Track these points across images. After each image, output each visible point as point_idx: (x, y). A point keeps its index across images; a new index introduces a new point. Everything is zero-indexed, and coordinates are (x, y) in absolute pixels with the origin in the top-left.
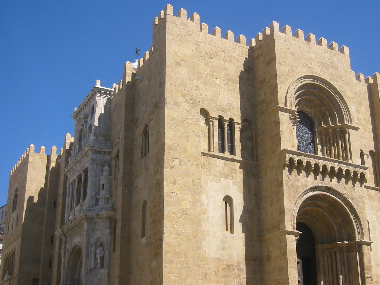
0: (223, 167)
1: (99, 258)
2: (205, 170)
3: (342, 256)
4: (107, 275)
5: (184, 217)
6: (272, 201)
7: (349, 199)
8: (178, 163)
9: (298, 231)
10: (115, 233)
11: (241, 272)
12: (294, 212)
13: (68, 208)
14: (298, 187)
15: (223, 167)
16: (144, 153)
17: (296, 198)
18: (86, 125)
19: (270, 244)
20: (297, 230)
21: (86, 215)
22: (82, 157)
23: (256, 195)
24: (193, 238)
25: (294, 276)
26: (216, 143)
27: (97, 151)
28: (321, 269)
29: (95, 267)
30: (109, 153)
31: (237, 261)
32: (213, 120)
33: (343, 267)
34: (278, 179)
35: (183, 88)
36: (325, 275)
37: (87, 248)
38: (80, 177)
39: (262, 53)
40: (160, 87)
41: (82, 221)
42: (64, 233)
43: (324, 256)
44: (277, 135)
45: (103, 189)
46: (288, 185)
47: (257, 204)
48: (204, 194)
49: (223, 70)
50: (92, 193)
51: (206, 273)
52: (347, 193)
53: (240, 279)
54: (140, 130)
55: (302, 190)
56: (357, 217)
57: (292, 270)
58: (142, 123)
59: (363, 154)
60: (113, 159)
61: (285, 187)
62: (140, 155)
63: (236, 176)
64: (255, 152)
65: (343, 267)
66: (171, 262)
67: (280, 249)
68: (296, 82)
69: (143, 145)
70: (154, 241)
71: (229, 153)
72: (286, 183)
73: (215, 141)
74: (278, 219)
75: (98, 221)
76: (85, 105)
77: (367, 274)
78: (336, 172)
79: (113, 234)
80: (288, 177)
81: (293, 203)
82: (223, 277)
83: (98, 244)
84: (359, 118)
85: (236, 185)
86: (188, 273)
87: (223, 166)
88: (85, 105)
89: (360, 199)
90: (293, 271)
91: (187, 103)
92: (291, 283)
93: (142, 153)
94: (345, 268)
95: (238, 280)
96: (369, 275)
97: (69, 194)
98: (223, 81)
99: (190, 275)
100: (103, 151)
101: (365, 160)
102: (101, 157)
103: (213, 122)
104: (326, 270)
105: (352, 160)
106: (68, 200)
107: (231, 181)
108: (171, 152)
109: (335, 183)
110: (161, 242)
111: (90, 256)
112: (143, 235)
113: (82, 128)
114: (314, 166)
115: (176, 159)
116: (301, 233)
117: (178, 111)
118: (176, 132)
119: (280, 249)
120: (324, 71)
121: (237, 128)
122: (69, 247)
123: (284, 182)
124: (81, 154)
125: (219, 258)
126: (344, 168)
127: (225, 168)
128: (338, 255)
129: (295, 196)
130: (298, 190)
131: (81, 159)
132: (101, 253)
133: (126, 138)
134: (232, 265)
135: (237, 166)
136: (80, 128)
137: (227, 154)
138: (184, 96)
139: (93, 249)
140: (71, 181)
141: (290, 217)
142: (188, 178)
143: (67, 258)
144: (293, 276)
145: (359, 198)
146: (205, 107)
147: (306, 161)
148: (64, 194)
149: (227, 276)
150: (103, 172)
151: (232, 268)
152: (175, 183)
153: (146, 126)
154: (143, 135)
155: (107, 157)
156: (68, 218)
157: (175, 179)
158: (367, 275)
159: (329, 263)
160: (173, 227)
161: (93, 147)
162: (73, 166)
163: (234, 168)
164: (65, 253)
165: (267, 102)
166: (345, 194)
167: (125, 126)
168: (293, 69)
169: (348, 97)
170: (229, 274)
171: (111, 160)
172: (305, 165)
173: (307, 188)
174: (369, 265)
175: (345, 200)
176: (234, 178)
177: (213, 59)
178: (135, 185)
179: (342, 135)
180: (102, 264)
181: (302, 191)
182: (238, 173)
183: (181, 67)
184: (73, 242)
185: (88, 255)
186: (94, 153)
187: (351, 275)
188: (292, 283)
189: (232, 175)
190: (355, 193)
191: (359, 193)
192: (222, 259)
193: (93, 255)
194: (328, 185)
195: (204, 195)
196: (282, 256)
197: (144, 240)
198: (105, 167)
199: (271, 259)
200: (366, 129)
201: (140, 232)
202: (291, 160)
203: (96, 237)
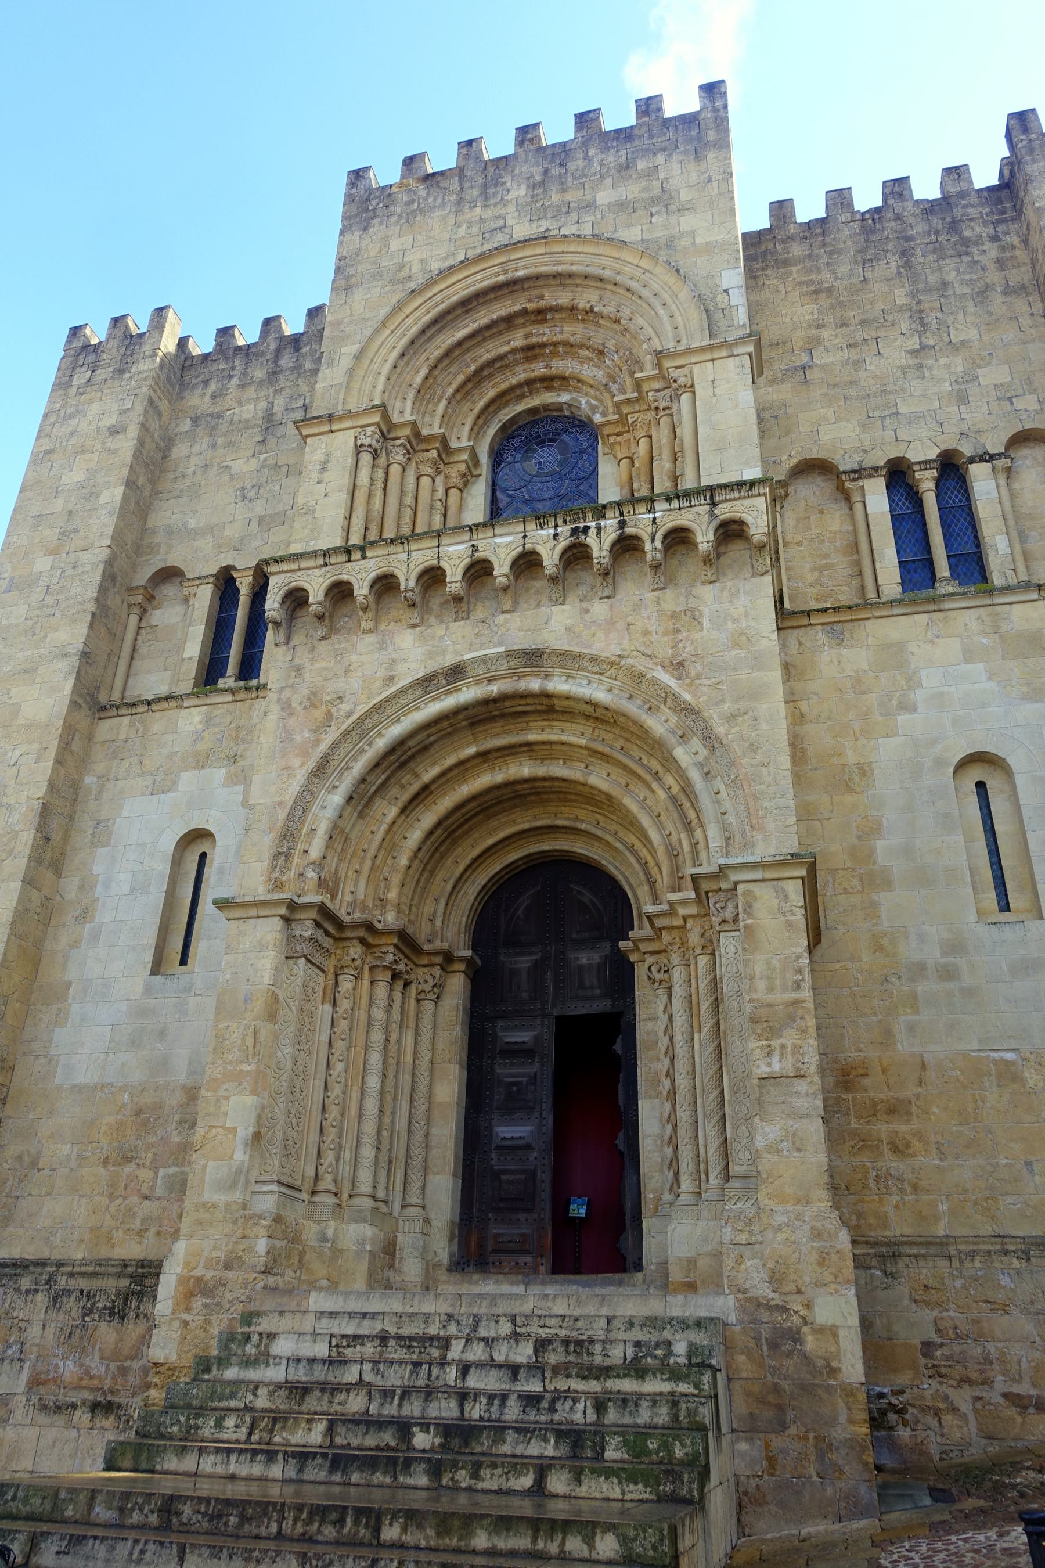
2: (126, 764)
14: (340, 698)
25: (229, 1124)
31: (183, 1087)
32: (192, 590)
46: (286, 707)
51: (39, 1153)
52: (642, 649)
53: (183, 1165)
55: (359, 707)
57: (225, 1094)
63: (245, 750)
68: (408, 310)
72: (279, 700)
73: (186, 655)
80: (293, 674)
81: (300, 776)
82: (106, 1161)
89: (734, 653)
90: (227, 1098)
92: (205, 1167)
95: (172, 1170)
109: (569, 622)
127: (206, 734)
128: (678, 975)
129: (317, 742)
130: (338, 710)
138: (54, 552)
145: (737, 645)
146: (173, 559)
158: (769, 1065)
166: (625, 653)
170: (136, 1147)
173: (393, 689)
176: (234, 759)
181: (361, 710)
191: (730, 623)
194: (522, 641)
195: (102, 851)
202: (296, 599)
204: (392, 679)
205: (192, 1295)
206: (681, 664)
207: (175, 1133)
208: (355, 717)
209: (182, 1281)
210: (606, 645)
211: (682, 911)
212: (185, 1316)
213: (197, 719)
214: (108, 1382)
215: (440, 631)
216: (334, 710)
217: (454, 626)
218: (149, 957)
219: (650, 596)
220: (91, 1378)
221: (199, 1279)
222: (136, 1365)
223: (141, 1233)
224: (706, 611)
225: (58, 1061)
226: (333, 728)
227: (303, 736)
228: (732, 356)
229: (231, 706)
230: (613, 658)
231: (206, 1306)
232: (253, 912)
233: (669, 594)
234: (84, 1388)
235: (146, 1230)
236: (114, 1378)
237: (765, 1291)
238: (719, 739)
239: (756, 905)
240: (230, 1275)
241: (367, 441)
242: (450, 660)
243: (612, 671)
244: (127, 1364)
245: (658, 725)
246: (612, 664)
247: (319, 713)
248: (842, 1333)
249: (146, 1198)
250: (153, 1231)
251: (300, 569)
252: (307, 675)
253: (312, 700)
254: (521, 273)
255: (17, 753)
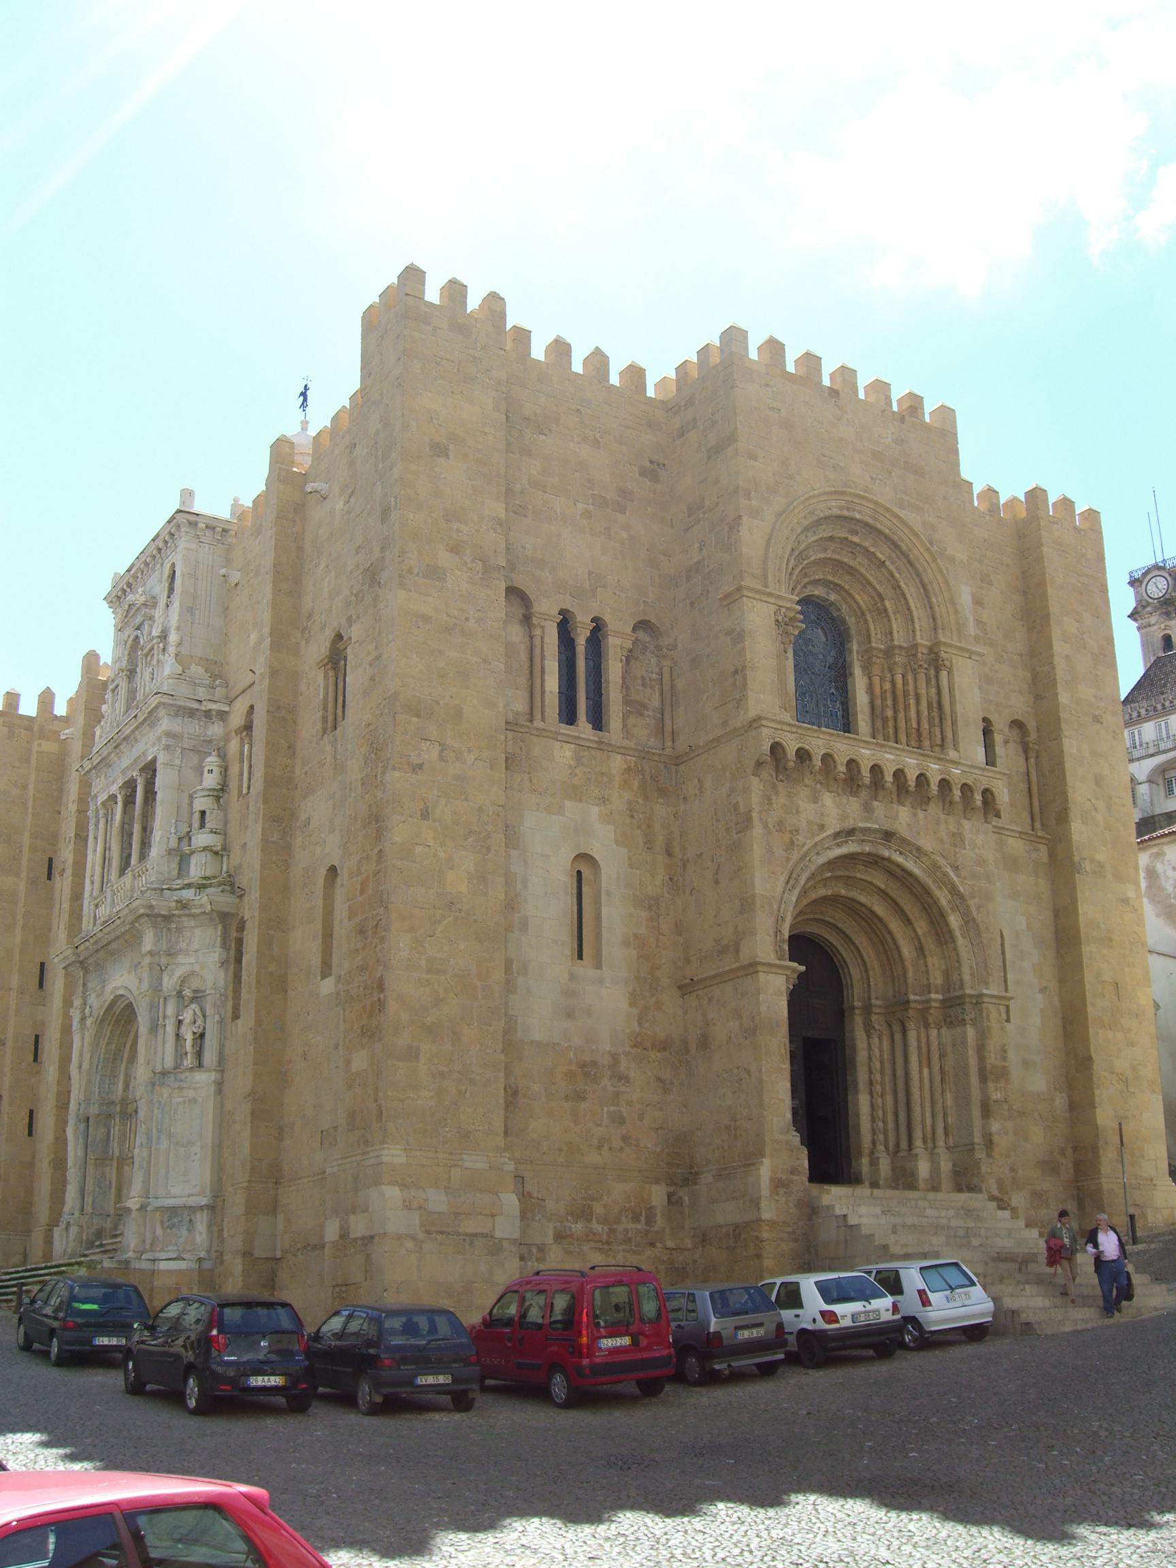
0: (570, 766)
1: (189, 1037)
3: (924, 1040)
4: (212, 1088)
5: (451, 918)
6: (717, 873)
7: (949, 867)
8: (437, 753)
9: (795, 964)
10: (239, 960)
11: (623, 1085)
12: (783, 904)
13: (92, 883)
14: (797, 831)
15: (570, 766)
16: (330, 718)
17: (791, 863)
18: (151, 626)
19: (710, 1000)
20: (790, 961)
21: (151, 907)
22: (137, 728)
23: (669, 853)
24: (479, 984)
25: (780, 1097)
26: (551, 692)
27: (184, 708)
28: (862, 1076)
29: (177, 1066)
30: (223, 715)
33: (926, 1070)
34: (736, 807)
35: (455, 525)
36: (871, 1093)
37: (153, 1006)
38: (130, 785)
39: (695, 420)
40: (383, 521)
41: (137, 925)
42: (81, 959)
43: (868, 1037)
44: (736, 672)
45: (202, 825)
46: (765, 826)
47: (671, 879)
48: (514, 849)
49: (577, 471)
50: (168, 838)
51: (518, 1088)
54: (318, 648)
56: (969, 921)
58: (323, 627)
59: (991, 730)
60: (233, 734)
61: (757, 830)
62: (319, 725)
64: (668, 723)
65: (926, 1070)
66: (412, 1054)
67: (739, 1016)
69: (326, 693)
70: (361, 989)
71: (591, 726)
72: (761, 819)
73: (547, 688)
74: (736, 927)
75: (186, 924)
76: (147, 564)
77: (996, 1090)
78: (910, 786)
79: (232, 967)
81: (782, 879)
82: (567, 1098)
83: (187, 993)
84: (981, 622)
85: (608, 823)
86: (463, 1088)
87: (572, 762)
88: (147, 564)
89: (979, 868)
91: (466, 570)
93: (325, 719)
94: (930, 1073)
95: (612, 1108)
96: (1001, 1093)
97: (96, 838)
98: (575, 504)
99: (468, 1094)
100: (203, 708)
101: (996, 748)
102: (197, 727)
103: (543, 628)
104: (878, 1076)
105: (959, 752)
106: (94, 858)
107: (595, 811)
108: (415, 720)
110: (382, 996)
111: (160, 1031)
112: (326, 969)
113: (137, 637)
114: (844, 767)
115: (428, 742)
116: (803, 968)
117: (436, 595)
118: (432, 659)
119: (739, 1016)
120: (881, 480)
121: (615, 645)
122: (97, 1004)
123: (755, 815)
124: (135, 717)
125: (558, 1041)
126: (934, 771)
127: (577, 771)
128: (912, 1035)
129: (788, 859)
130: (798, 840)
131: (133, 732)
132: (195, 1022)
133: (274, 673)
134: (594, 1064)
135: (612, 765)
136: (132, 637)
137: (584, 726)
138: (456, 549)
139: (171, 1009)
140: (103, 797)
141: (771, 921)
142: (466, 799)
143: (89, 1036)
144: (778, 1099)
147: (823, 752)
148: (81, 839)
149: (580, 1097)
150: (202, 775)
151: (595, 1073)
152: (425, 814)
153: (339, 637)
154: (327, 664)
155: (216, 730)
156: (92, 915)
157: (425, 803)
159: (886, 1056)
160: (420, 948)
161: (172, 695)
162: (110, 754)
163: (604, 771)
164: (83, 1019)
165: (707, 570)
167: (271, 634)
168: (790, 473)
169: (952, 560)
170: (586, 1090)
171: (226, 739)
172: (819, 763)
173: (825, 834)
174: (1002, 1064)
175: (936, 867)
176: (604, 801)
177: (546, 435)
178: (303, 816)
179: (932, 672)
180: (199, 1054)
181: (810, 843)
182: (617, 786)
183: (448, 458)
184: (109, 988)
185: (154, 1028)
186: (177, 715)
187: (949, 1096)
188: (775, 1118)
189: (597, 791)
190: (965, 849)
192: (566, 1045)
193: (170, 1029)
196: (746, 1038)
197: (328, 986)
198: (208, 759)
199: (712, 1047)
200: (1002, 657)
201: (316, 961)
202: (776, 748)
203: (179, 972)
204: (822, 827)
205: (778, 1187)
206: (957, 867)
207: (609, 1084)
208: (805, 849)
209: (772, 1179)
210: (926, 843)
211: (933, 1004)
212: (776, 1198)
213: (569, 754)
214: (605, 1237)
215: (844, 799)
216: (794, 839)
217: (851, 798)
218: (568, 952)
219: (942, 817)
220: (594, 1234)
221: (780, 1180)
222: (620, 1228)
223: (600, 1147)
224: (966, 837)
225: (516, 1021)
226: (795, 852)
227: (779, 852)
228: (970, 658)
229: (593, 752)
230: (929, 853)
231: (785, 1192)
232: (774, 970)
233: (951, 819)
234: (591, 1240)
235: (603, 1146)
236: (608, 1236)
237: (996, 1192)
238: (974, 919)
239: (991, 1016)
240: (795, 1178)
241: (780, 619)
242: (849, 824)
243: (924, 859)
244: (615, 1227)
245: (943, 898)
246: (927, 855)
247: (787, 836)
248: (1020, 1210)
249: (599, 1125)
250: (606, 1147)
251: (781, 730)
252: (774, 806)
253: (780, 824)
254: (857, 516)
255: (470, 758)
